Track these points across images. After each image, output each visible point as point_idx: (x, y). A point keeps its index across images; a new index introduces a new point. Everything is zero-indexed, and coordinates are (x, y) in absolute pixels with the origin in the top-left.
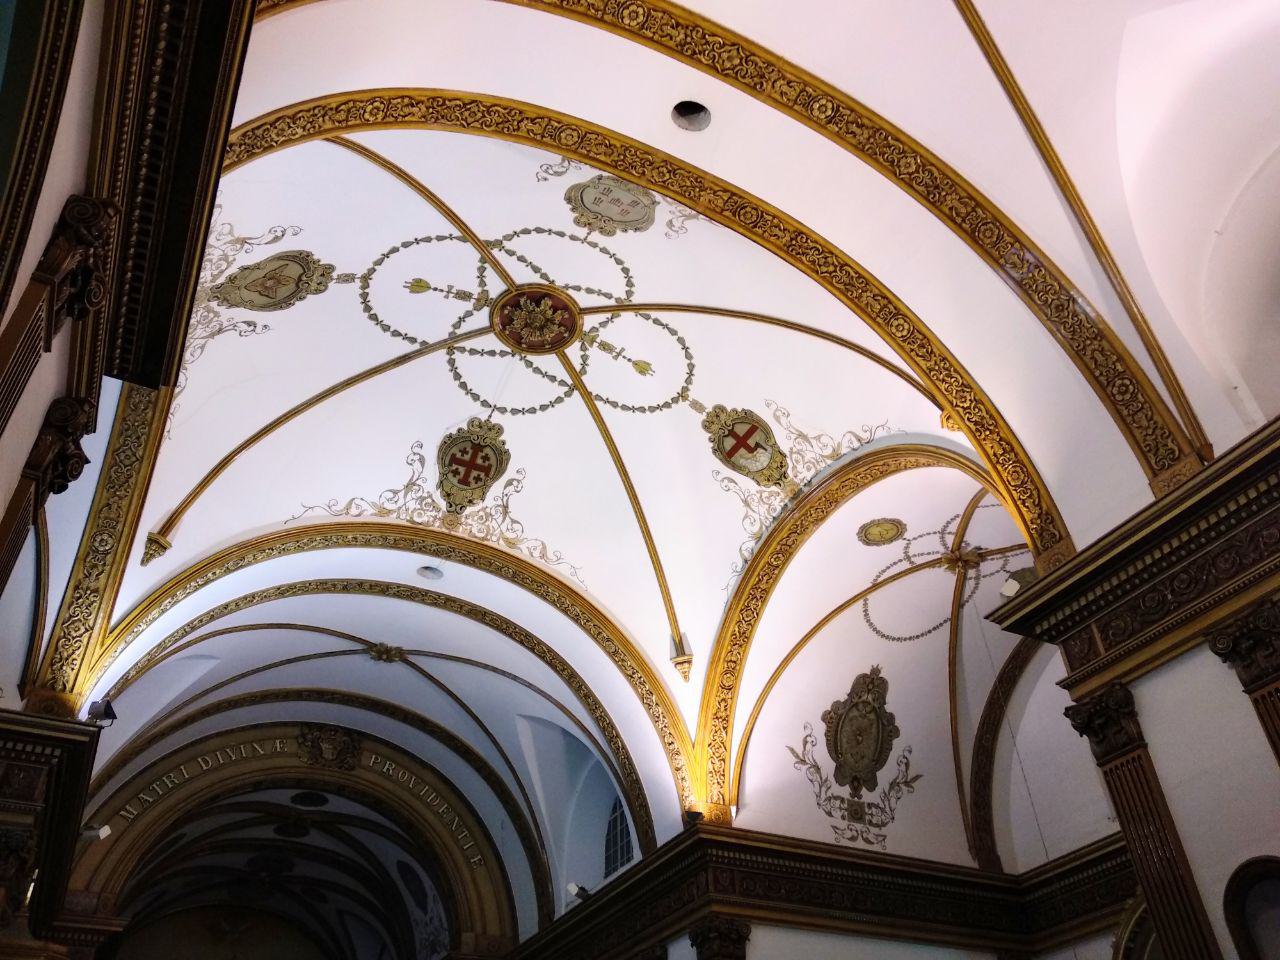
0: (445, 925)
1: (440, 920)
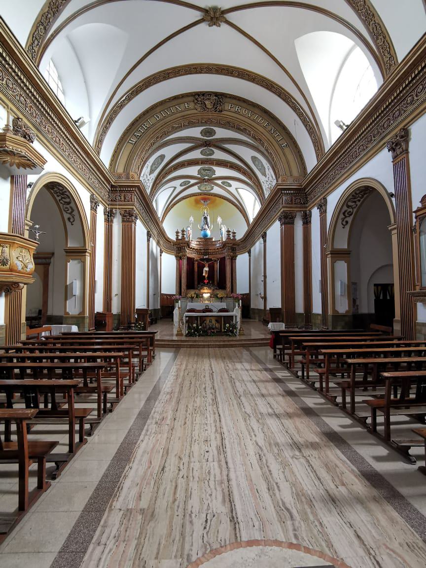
0: (274, 178)
1: (272, 177)
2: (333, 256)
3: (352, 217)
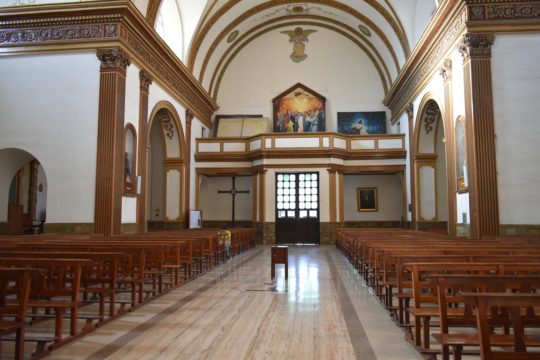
2: (419, 161)
3: (435, 123)
